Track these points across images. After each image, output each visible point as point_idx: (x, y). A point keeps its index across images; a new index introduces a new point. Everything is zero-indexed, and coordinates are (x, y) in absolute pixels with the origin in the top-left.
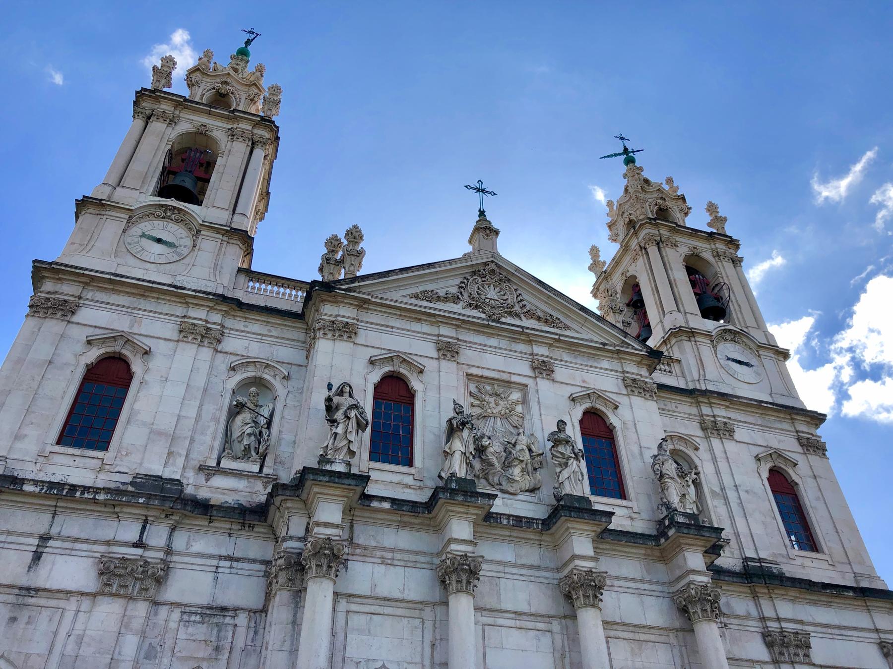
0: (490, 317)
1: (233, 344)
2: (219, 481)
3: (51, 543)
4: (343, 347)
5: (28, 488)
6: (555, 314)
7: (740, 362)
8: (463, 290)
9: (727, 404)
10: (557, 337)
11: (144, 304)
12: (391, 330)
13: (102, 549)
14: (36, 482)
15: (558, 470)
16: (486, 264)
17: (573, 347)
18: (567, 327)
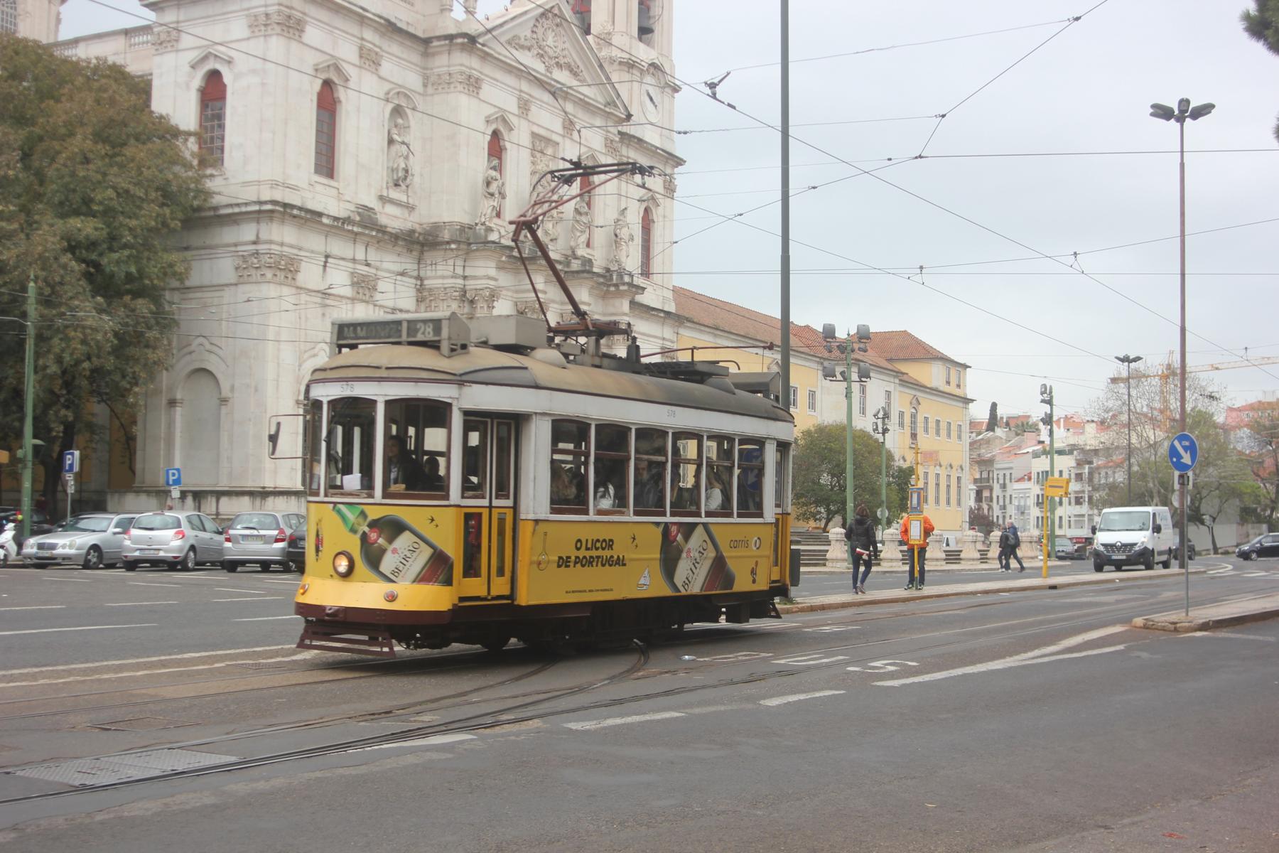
0: (547, 70)
1: (387, 67)
2: (390, 209)
3: (330, 260)
4: (474, 102)
5: (325, 220)
6: (582, 67)
7: (651, 99)
8: (535, 36)
9: (637, 146)
10: (582, 97)
11: (338, 22)
12: (495, 82)
13: (350, 265)
14: (329, 216)
15: (578, 234)
16: (553, 7)
17: (585, 104)
18: (583, 81)
